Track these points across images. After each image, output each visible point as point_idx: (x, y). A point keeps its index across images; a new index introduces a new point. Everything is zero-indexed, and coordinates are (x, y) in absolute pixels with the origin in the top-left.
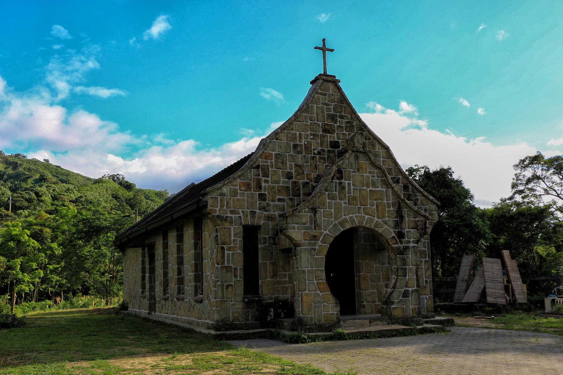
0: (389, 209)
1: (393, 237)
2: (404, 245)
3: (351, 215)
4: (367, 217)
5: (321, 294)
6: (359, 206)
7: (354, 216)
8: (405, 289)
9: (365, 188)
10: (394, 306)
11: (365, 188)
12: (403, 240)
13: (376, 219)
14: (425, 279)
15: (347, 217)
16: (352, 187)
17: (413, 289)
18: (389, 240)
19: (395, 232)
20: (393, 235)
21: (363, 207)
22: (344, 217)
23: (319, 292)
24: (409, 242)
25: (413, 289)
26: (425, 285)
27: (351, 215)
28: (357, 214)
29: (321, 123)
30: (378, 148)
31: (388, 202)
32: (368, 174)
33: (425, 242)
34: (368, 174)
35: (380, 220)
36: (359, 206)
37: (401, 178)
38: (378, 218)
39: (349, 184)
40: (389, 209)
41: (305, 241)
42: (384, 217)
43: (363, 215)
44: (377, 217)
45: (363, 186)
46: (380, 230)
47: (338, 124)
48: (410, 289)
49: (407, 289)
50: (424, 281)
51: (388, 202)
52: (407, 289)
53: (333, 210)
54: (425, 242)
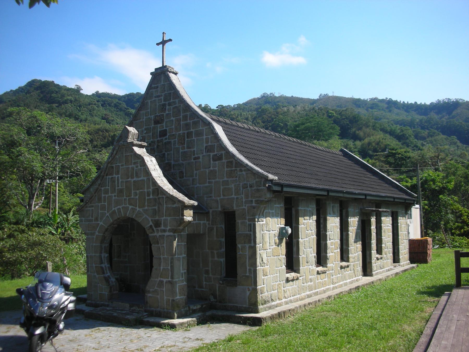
0: (149, 198)
1: (151, 226)
2: (160, 234)
3: (118, 207)
4: (130, 207)
5: (97, 276)
6: (125, 197)
7: (121, 207)
8: (159, 279)
9: (130, 179)
10: (150, 295)
11: (130, 179)
12: (159, 229)
13: (138, 209)
14: (248, 268)
15: (116, 209)
16: (120, 180)
17: (167, 280)
18: (146, 229)
19: (152, 220)
20: (151, 223)
21: (128, 198)
22: (113, 209)
23: (96, 274)
24: (164, 231)
25: (167, 280)
26: (248, 274)
27: (118, 207)
28: (123, 205)
29: (153, 116)
30: (201, 127)
31: (148, 190)
32: (133, 166)
33: (251, 224)
34: (133, 166)
35: (141, 210)
36: (125, 197)
37: (224, 153)
38: (139, 207)
39: (118, 177)
40: (149, 198)
41: (89, 232)
42: (144, 206)
43: (128, 205)
44: (139, 207)
45: (128, 178)
46: (140, 220)
47: (167, 112)
48: (165, 280)
49: (162, 279)
50: (248, 270)
51: (148, 190)
52: (162, 279)
53: (106, 204)
54: (251, 224)
